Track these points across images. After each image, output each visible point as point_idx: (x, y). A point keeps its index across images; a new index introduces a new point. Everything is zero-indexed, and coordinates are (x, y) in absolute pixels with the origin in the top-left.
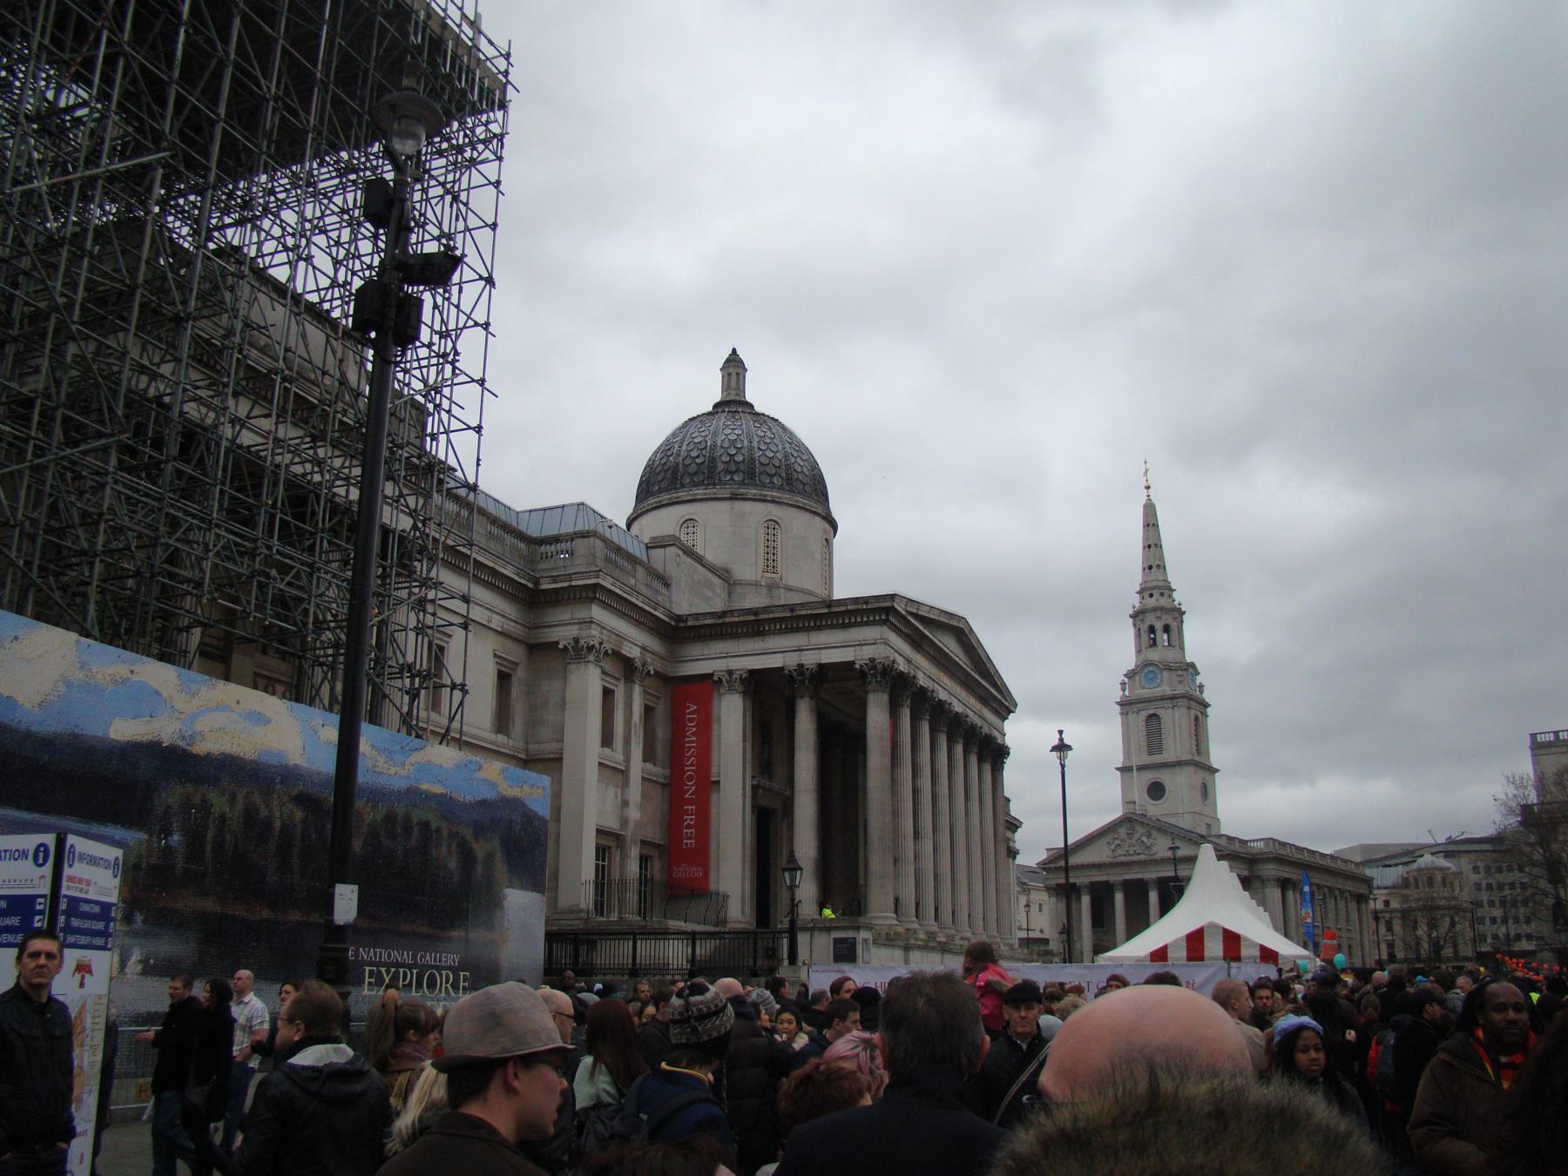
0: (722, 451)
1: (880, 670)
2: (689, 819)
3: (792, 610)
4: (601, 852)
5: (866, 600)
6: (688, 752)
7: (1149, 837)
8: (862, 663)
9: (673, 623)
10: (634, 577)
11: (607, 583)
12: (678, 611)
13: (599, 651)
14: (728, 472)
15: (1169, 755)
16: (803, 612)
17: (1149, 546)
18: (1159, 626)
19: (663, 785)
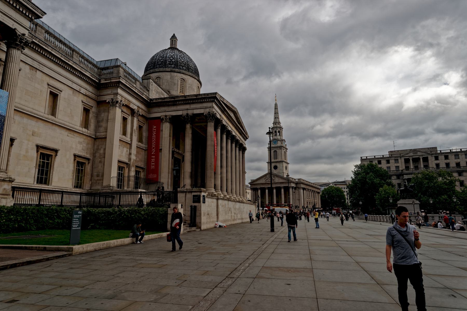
0: (169, 58)
1: (211, 116)
2: (153, 160)
3: (185, 97)
4: (120, 168)
5: (208, 94)
6: (153, 140)
7: (274, 177)
8: (206, 113)
9: (149, 101)
10: (136, 84)
11: (123, 82)
12: (151, 98)
13: (120, 104)
14: (170, 64)
15: (279, 159)
16: (189, 98)
17: (276, 113)
18: (277, 131)
19: (145, 150)
